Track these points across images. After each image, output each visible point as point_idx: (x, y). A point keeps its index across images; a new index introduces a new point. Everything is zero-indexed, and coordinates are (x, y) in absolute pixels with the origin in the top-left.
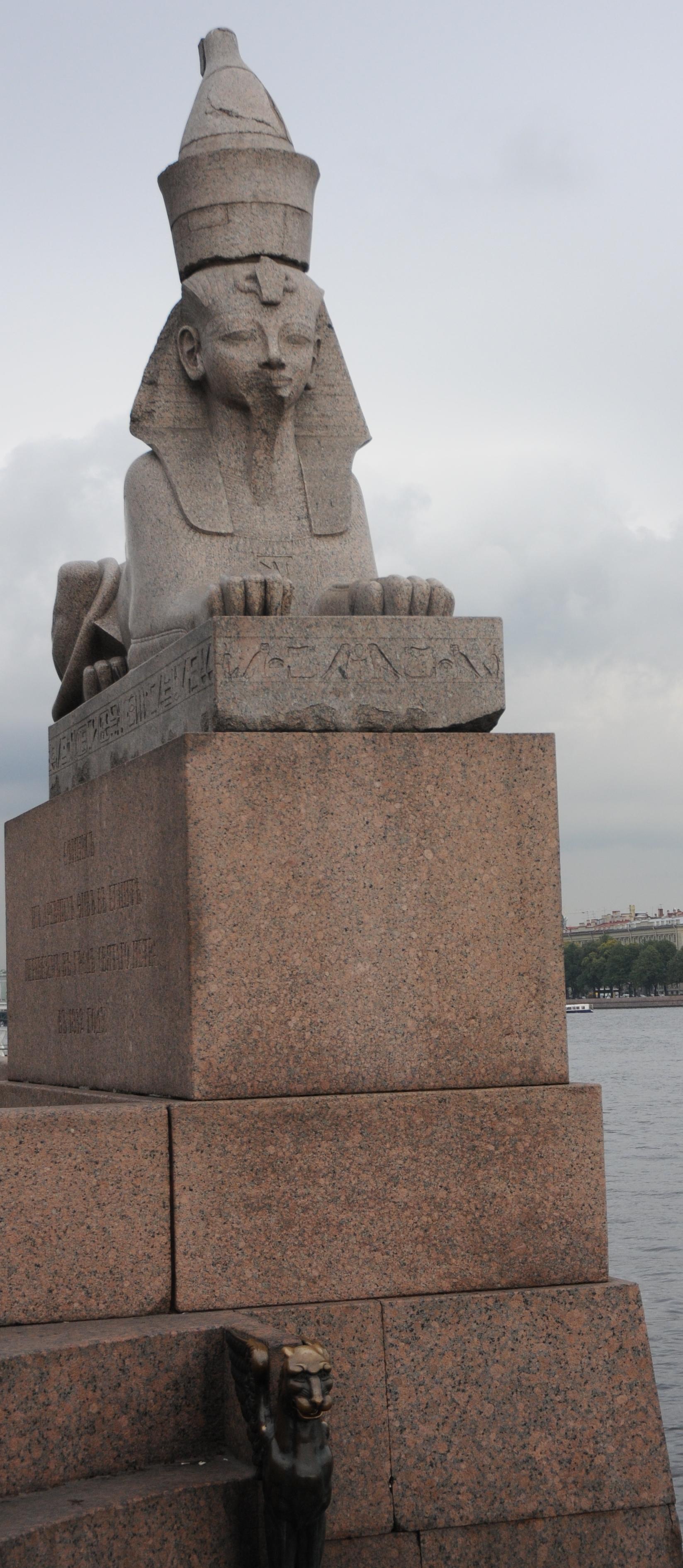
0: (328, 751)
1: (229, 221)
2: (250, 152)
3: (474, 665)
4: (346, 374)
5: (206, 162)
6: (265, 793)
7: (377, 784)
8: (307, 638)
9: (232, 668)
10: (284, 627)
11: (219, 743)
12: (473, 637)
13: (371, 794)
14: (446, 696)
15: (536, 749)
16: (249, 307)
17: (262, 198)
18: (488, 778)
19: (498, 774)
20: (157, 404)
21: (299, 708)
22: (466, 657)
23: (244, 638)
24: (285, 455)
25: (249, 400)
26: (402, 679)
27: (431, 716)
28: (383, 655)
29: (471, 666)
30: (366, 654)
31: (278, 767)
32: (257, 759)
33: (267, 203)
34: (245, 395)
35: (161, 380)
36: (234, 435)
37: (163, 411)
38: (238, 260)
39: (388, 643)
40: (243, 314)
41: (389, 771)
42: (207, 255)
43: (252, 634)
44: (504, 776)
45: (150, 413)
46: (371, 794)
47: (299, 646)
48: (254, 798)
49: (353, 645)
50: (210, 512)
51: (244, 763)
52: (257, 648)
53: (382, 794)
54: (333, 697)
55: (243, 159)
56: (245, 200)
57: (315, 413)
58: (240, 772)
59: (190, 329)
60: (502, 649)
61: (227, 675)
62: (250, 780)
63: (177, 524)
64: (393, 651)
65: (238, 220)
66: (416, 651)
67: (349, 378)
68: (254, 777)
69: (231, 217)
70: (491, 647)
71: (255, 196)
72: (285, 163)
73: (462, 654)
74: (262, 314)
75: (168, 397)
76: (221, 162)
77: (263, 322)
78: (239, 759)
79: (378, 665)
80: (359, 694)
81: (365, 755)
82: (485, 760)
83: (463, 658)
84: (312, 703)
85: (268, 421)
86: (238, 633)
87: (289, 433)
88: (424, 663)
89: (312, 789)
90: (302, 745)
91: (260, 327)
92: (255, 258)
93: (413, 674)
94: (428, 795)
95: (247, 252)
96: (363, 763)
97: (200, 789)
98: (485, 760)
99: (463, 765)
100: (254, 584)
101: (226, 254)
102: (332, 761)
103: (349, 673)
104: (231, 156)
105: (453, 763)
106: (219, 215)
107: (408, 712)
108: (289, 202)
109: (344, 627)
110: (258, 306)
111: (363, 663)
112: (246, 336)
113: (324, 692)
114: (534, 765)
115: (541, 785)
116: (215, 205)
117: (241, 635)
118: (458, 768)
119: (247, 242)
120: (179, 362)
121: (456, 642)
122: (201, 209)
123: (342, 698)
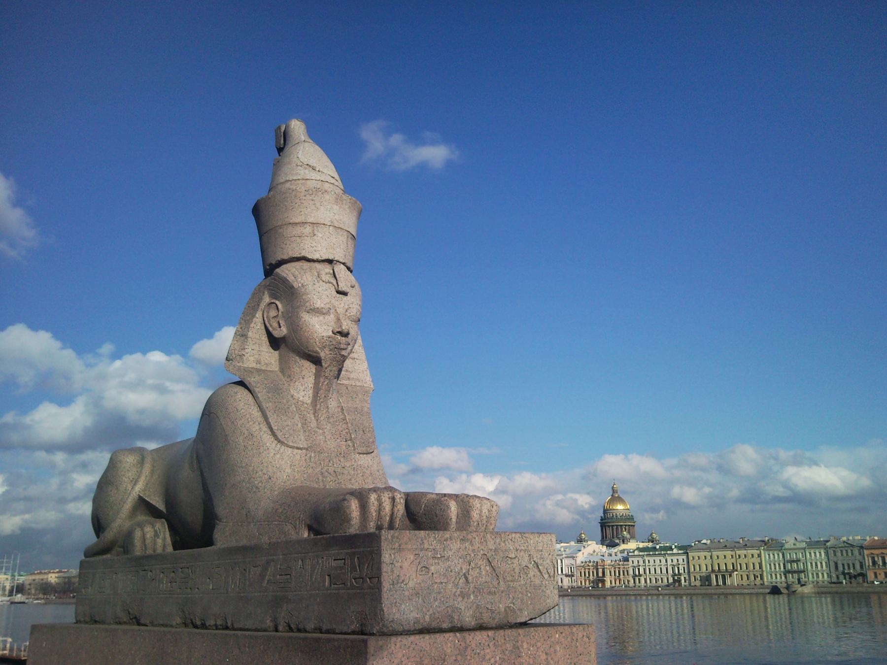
0: (466, 648)
5: (303, 194)
14: (527, 595)
17: (336, 224)
20: (247, 351)
21: (439, 610)
25: (322, 355)
26: (502, 583)
27: (518, 612)
29: (540, 571)
35: (250, 334)
38: (318, 261)
42: (297, 255)
43: (410, 547)
45: (242, 356)
50: (291, 431)
54: (460, 599)
59: (277, 302)
63: (267, 438)
65: (320, 235)
75: (254, 347)
77: (336, 304)
80: (476, 596)
81: (488, 651)
84: (447, 605)
88: (514, 570)
92: (330, 262)
96: (487, 657)
99: (546, 654)
103: (470, 578)
106: (308, 229)
107: (505, 610)
109: (468, 540)
111: (478, 570)
112: (324, 311)
113: (455, 595)
118: (543, 657)
119: (324, 250)
123: (466, 600)
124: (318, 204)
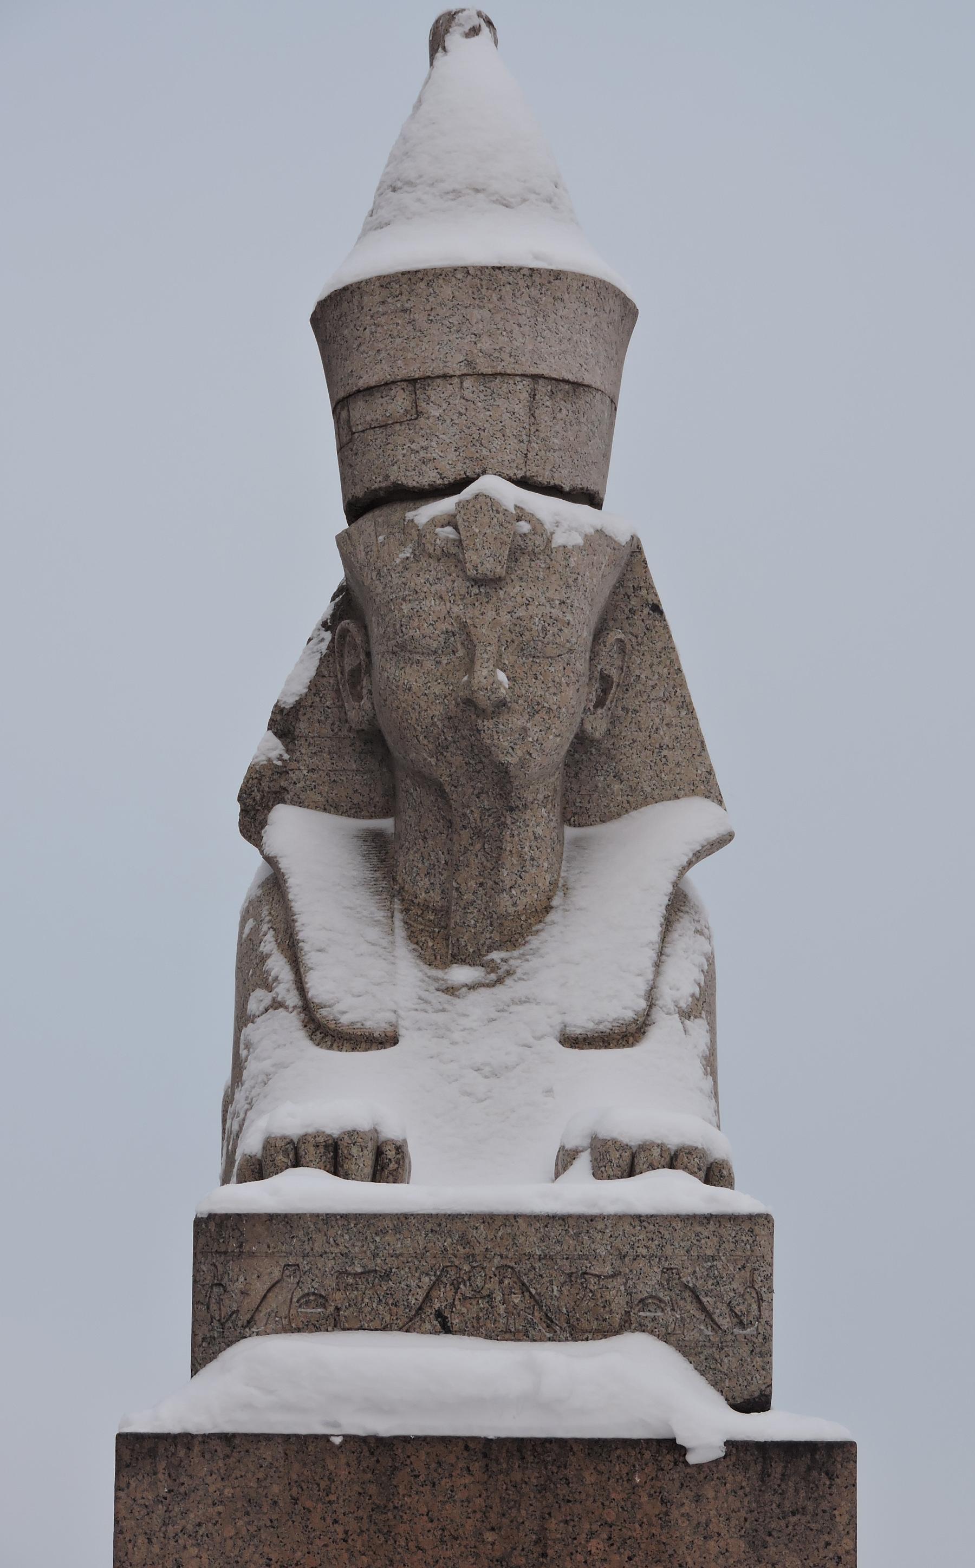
1: (419, 414)
2: (459, 275)
3: (710, 1308)
4: (687, 706)
5: (378, 298)
6: (266, 1549)
7: (490, 1537)
8: (375, 1256)
9: (225, 1311)
10: (331, 1232)
11: (182, 1453)
12: (709, 1252)
13: (477, 1555)
15: (815, 1473)
16: (441, 588)
17: (484, 366)
18: (713, 1528)
19: (734, 1522)
22: (693, 1291)
23: (252, 1255)
24: (526, 876)
28: (524, 1288)
29: (703, 1309)
30: (493, 1285)
31: (295, 1501)
32: (253, 1484)
33: (495, 375)
34: (433, 761)
36: (425, 839)
37: (304, 790)
39: (538, 1265)
40: (430, 603)
41: (514, 1512)
42: (378, 483)
44: (747, 1525)
46: (477, 1555)
47: (359, 1270)
48: (247, 1556)
49: (466, 1268)
51: (228, 1492)
52: (277, 1274)
53: (498, 1554)
55: (447, 291)
56: (447, 370)
57: (617, 787)
58: (220, 1508)
60: (769, 1277)
61: (216, 1324)
62: (240, 1523)
64: (546, 1279)
66: (593, 1280)
67: (691, 711)
68: (246, 1519)
69: (423, 405)
70: (746, 1274)
71: (469, 363)
72: (534, 292)
73: (686, 1286)
74: (468, 600)
76: (404, 298)
78: (219, 1485)
79: (515, 1306)
81: (467, 1480)
82: (711, 1494)
83: (687, 1294)
85: (484, 811)
86: (241, 1246)
87: (539, 831)
88: (607, 1303)
89: (359, 1544)
90: (343, 1461)
91: (464, 626)
93: (585, 1325)
94: (590, 1559)
95: (452, 475)
97: (141, 1540)
98: (711, 1494)
100: (312, 1149)
101: (411, 483)
102: (401, 1490)
104: (422, 285)
105: (645, 1499)
106: (399, 402)
108: (543, 369)
109: (450, 1233)
110: (460, 585)
114: (810, 1506)
115: (822, 1544)
116: (393, 382)
117: (246, 1248)
119: (452, 456)
120: (338, 691)
121: (676, 1263)
122: (369, 390)
124: (420, 318)
